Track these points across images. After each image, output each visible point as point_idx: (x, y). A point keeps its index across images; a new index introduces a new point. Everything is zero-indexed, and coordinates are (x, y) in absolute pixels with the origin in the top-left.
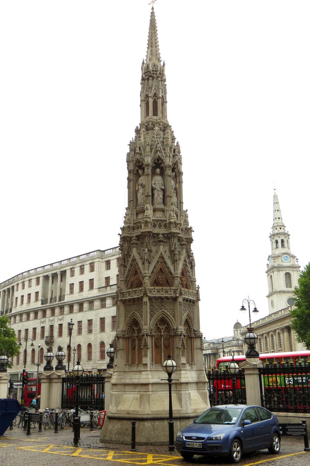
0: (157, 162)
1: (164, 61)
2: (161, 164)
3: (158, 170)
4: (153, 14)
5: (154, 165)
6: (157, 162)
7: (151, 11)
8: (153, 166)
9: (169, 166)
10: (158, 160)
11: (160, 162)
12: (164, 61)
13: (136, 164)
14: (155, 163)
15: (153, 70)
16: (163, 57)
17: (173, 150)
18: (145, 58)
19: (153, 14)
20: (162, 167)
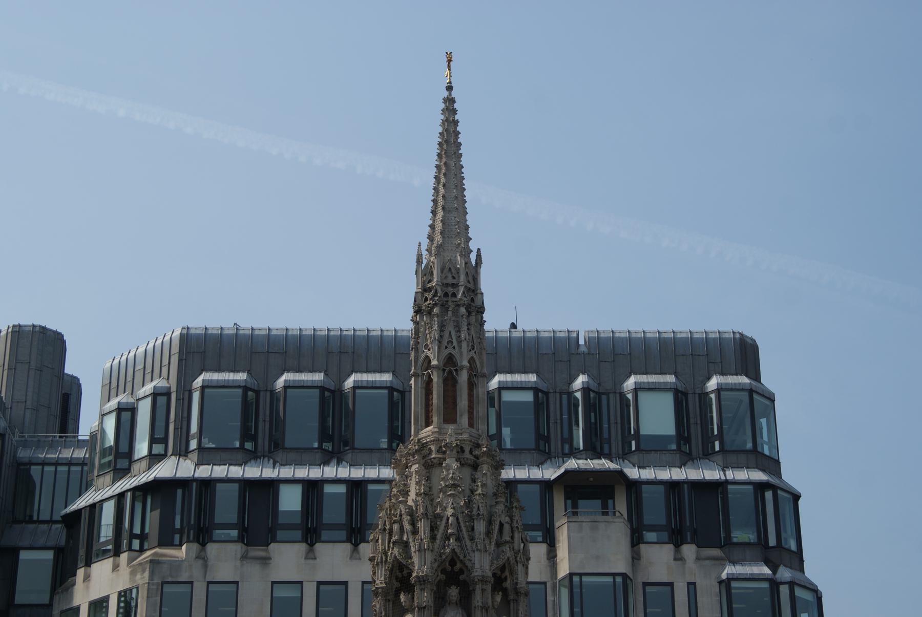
0: (449, 568)
1: (479, 250)
2: (461, 572)
3: (454, 592)
4: (450, 101)
5: (443, 577)
6: (449, 568)
7: (446, 94)
8: (440, 580)
9: (483, 580)
10: (453, 562)
11: (459, 566)
12: (479, 250)
13: (391, 571)
14: (443, 571)
15: (445, 282)
16: (480, 237)
17: (497, 528)
18: (425, 243)
19: (450, 101)
20: (465, 581)
